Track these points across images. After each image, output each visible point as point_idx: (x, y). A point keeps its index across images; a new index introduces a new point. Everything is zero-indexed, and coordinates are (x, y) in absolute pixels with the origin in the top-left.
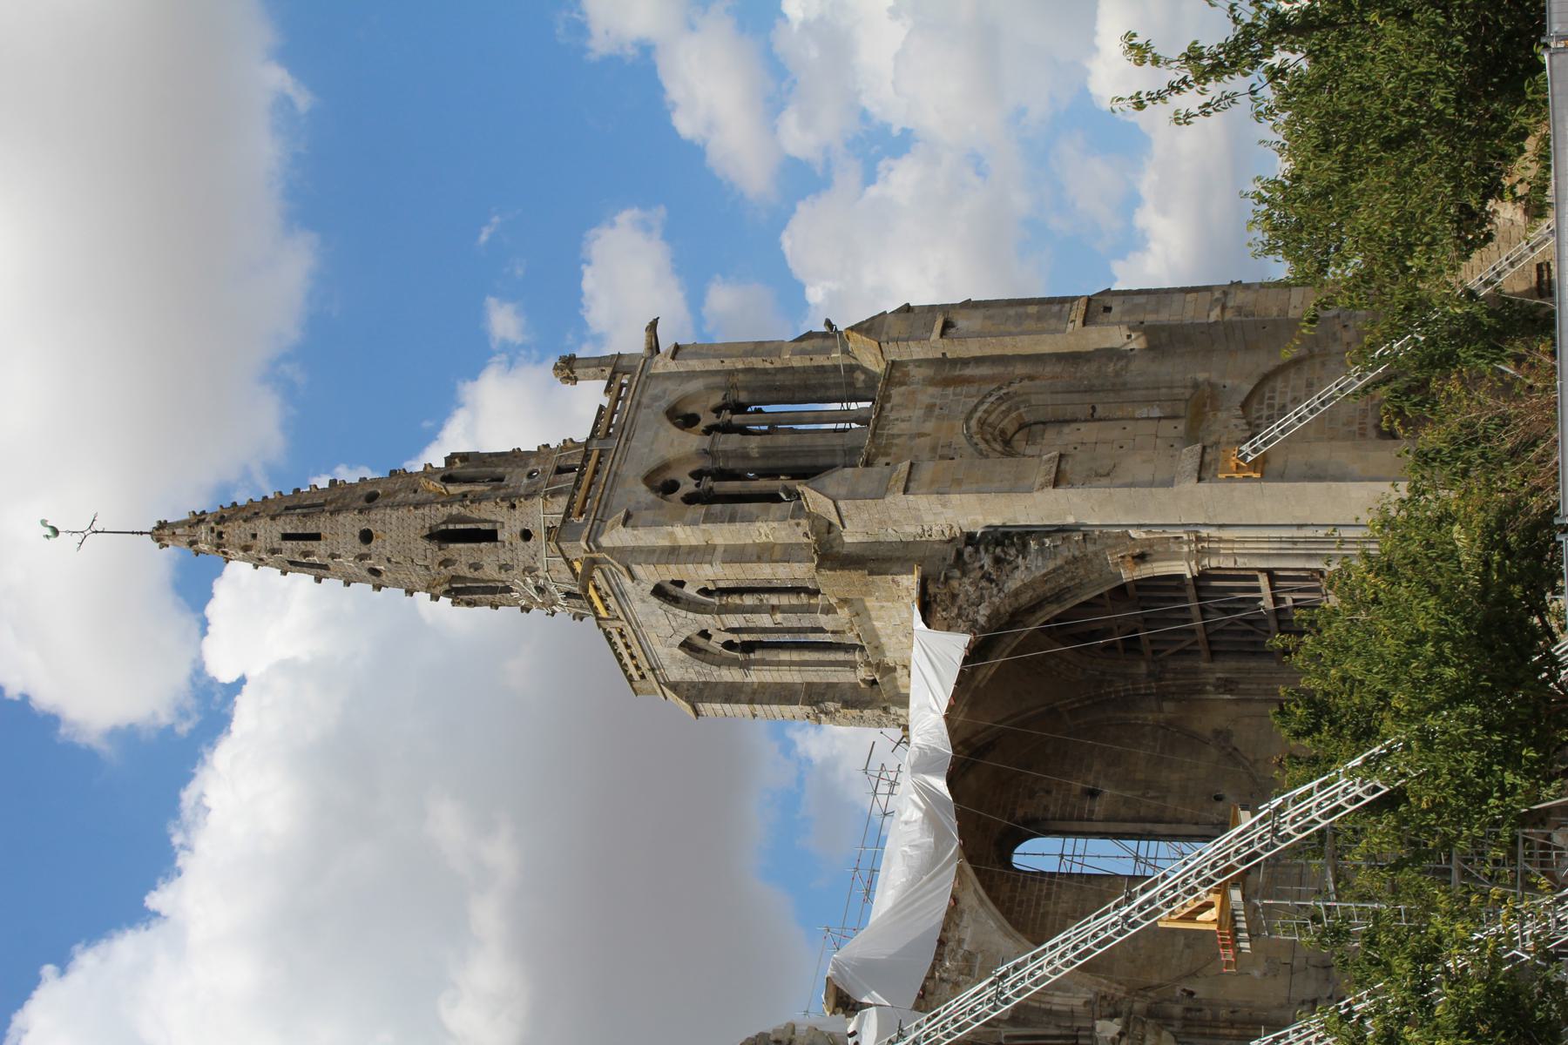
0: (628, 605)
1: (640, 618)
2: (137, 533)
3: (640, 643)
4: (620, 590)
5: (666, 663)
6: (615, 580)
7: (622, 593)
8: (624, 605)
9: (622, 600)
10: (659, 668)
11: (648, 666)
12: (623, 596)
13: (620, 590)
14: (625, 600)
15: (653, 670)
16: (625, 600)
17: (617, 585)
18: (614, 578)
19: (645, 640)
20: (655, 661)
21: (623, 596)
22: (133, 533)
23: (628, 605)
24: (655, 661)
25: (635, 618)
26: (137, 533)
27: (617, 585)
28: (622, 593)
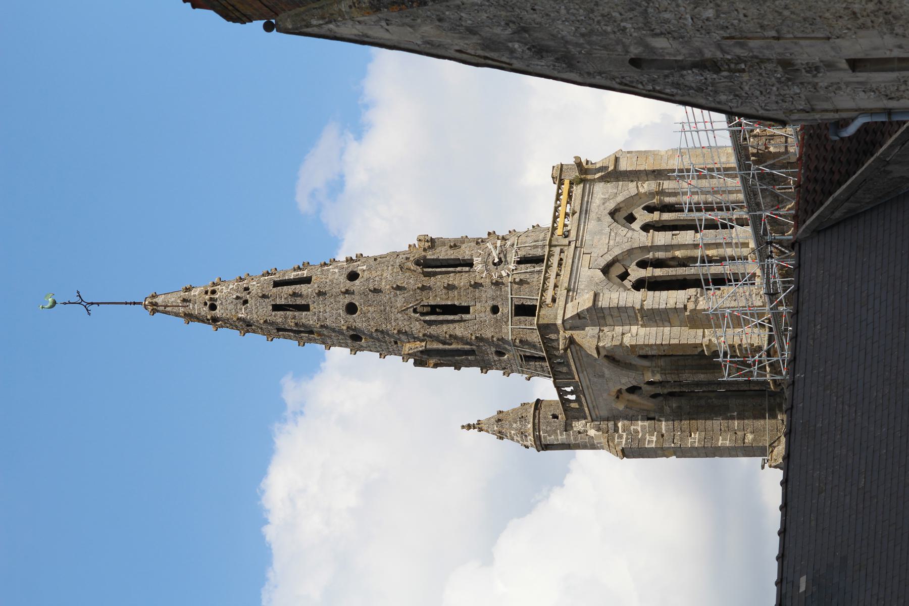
0: (585, 222)
1: (587, 237)
2: (131, 303)
3: (573, 262)
4: (587, 207)
5: (581, 286)
6: (588, 198)
7: (586, 211)
8: (583, 220)
9: (583, 216)
12: (586, 214)
13: (587, 207)
14: (585, 218)
16: (585, 218)
17: (588, 202)
18: (589, 196)
19: (579, 260)
20: (575, 283)
21: (586, 214)
22: (126, 303)
23: (585, 222)
24: (575, 283)
25: (583, 236)
26: (131, 303)
27: (588, 202)
28: (586, 211)
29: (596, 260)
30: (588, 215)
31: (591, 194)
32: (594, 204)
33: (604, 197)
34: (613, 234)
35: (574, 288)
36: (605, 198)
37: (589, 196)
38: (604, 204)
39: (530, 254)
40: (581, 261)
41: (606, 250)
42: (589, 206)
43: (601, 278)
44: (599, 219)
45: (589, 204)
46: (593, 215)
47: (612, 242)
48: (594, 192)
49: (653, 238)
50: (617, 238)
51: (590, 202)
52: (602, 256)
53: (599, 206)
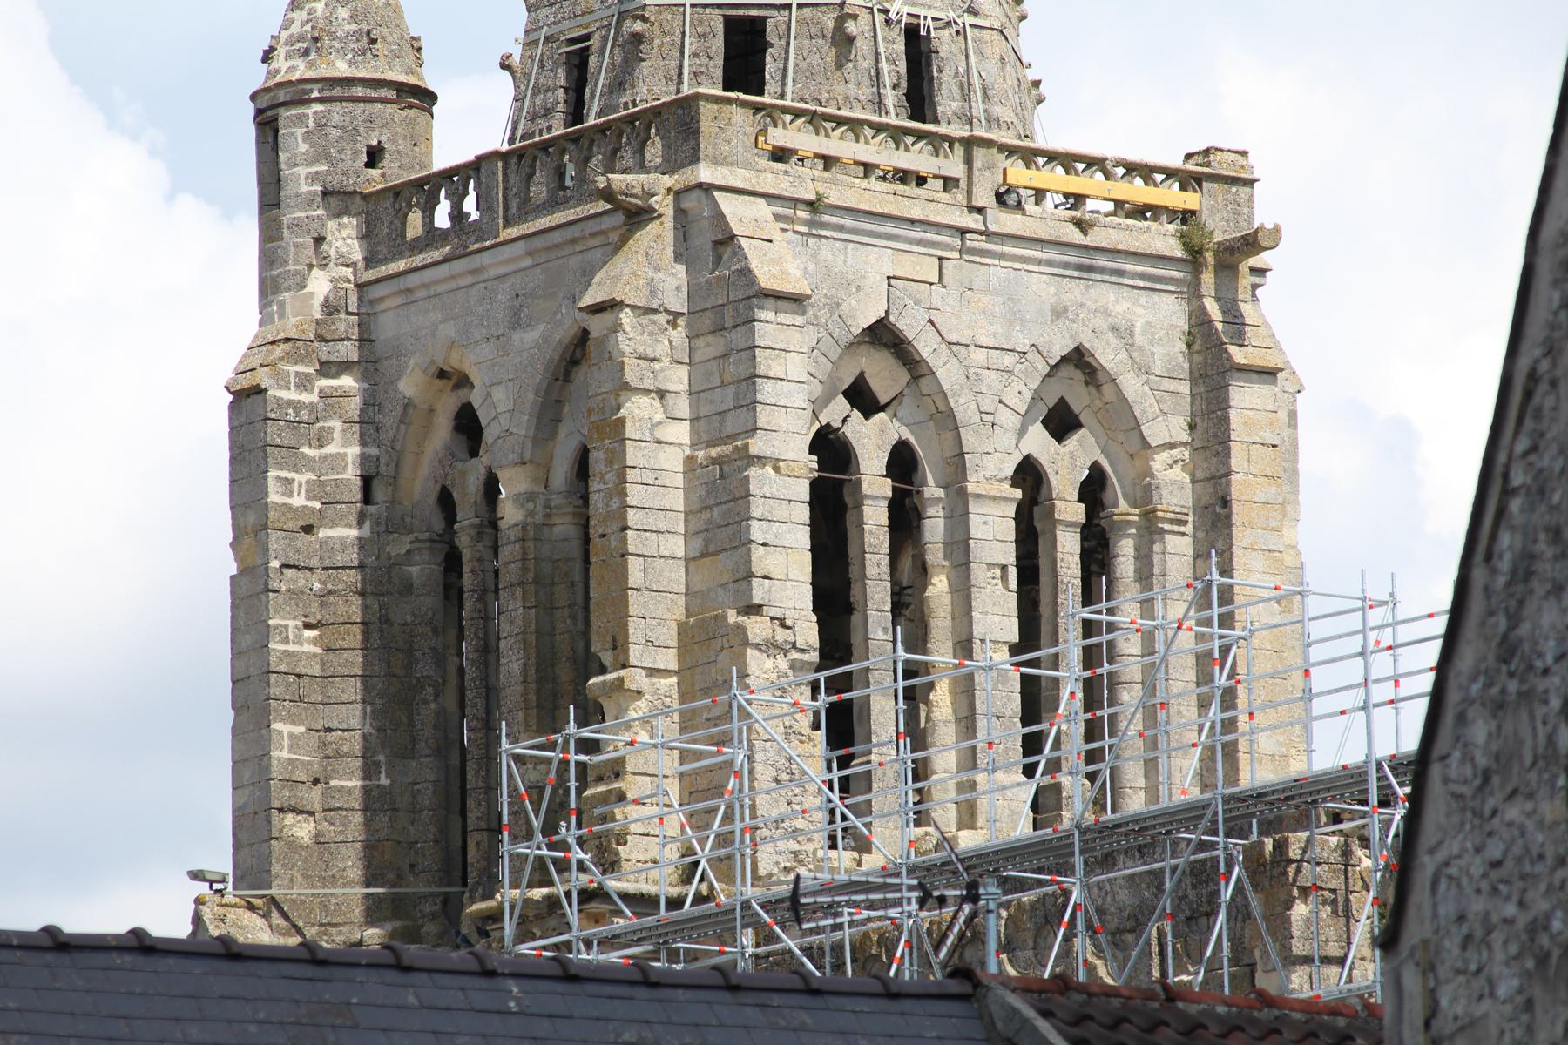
0: (1049, 263)
1: (998, 272)
3: (913, 222)
4: (1102, 270)
7: (1090, 269)
10: (810, 224)
11: (833, 198)
12: (1080, 267)
13: (1102, 270)
14: (1066, 265)
15: (813, 205)
16: (1066, 265)
17: (1120, 273)
18: (1142, 276)
19: (919, 242)
20: (841, 228)
21: (1080, 267)
23: (1049, 263)
24: (841, 228)
25: (1002, 256)
27: (1120, 273)
28: (1090, 269)
29: (918, 302)
30: (1076, 274)
31: (1148, 284)
32: (1112, 297)
33: (1137, 330)
34: (1008, 360)
35: (823, 225)
36: (1132, 335)
37: (1142, 276)
38: (1114, 329)
39: (940, 71)
40: (915, 248)
41: (953, 338)
42: (1106, 278)
43: (854, 318)
44: (1059, 312)
45: (1114, 279)
46: (1074, 291)
47: (979, 356)
48: (1156, 297)
49: (994, 498)
50: (993, 374)
51: (1121, 280)
52: (930, 321)
53: (1107, 313)
